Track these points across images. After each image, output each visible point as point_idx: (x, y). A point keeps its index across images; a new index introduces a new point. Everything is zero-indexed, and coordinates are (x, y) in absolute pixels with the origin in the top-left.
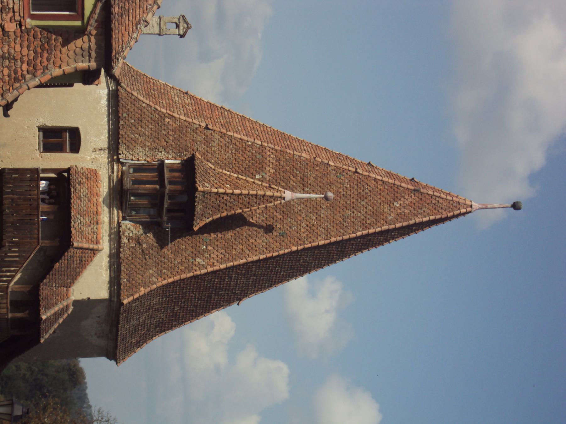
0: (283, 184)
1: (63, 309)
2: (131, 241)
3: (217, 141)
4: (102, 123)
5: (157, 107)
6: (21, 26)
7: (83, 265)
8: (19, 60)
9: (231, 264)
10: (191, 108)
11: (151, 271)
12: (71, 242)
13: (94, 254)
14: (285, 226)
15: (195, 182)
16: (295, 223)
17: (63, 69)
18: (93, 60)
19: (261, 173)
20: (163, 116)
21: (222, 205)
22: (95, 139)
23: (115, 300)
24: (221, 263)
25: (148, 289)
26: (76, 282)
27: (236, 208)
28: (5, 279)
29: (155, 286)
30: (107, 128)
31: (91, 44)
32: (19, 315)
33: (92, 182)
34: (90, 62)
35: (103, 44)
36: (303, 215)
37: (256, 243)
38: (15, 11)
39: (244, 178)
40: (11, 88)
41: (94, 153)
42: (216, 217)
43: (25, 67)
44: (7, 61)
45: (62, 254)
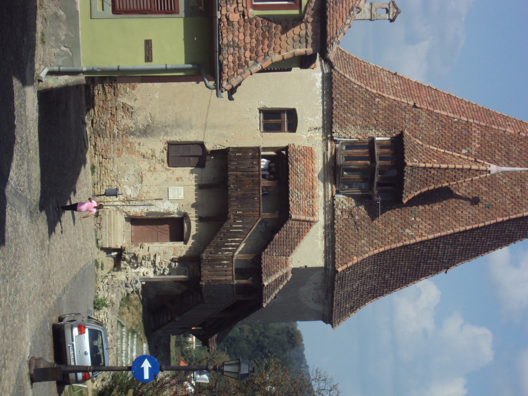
0: (489, 158)
1: (283, 276)
2: (344, 213)
3: (424, 119)
4: (317, 104)
5: (368, 88)
6: (244, 16)
7: (300, 235)
8: (242, 48)
9: (437, 235)
10: (399, 88)
11: (363, 241)
12: (289, 214)
13: (311, 226)
14: (491, 198)
15: (404, 158)
16: (500, 195)
17: (282, 54)
18: (309, 46)
19: (467, 148)
20: (373, 96)
21: (429, 179)
23: (331, 268)
24: (429, 234)
25: (361, 258)
26: (294, 251)
27: (442, 181)
28: (230, 248)
29: (367, 255)
31: (307, 30)
32: (243, 281)
33: (308, 159)
34: (306, 47)
35: (319, 31)
36: (508, 188)
37: (462, 215)
38: (239, 2)
39: (451, 153)
40: (236, 73)
41: (310, 132)
42: (423, 190)
43: (248, 54)
44: (232, 49)
45: (282, 226)
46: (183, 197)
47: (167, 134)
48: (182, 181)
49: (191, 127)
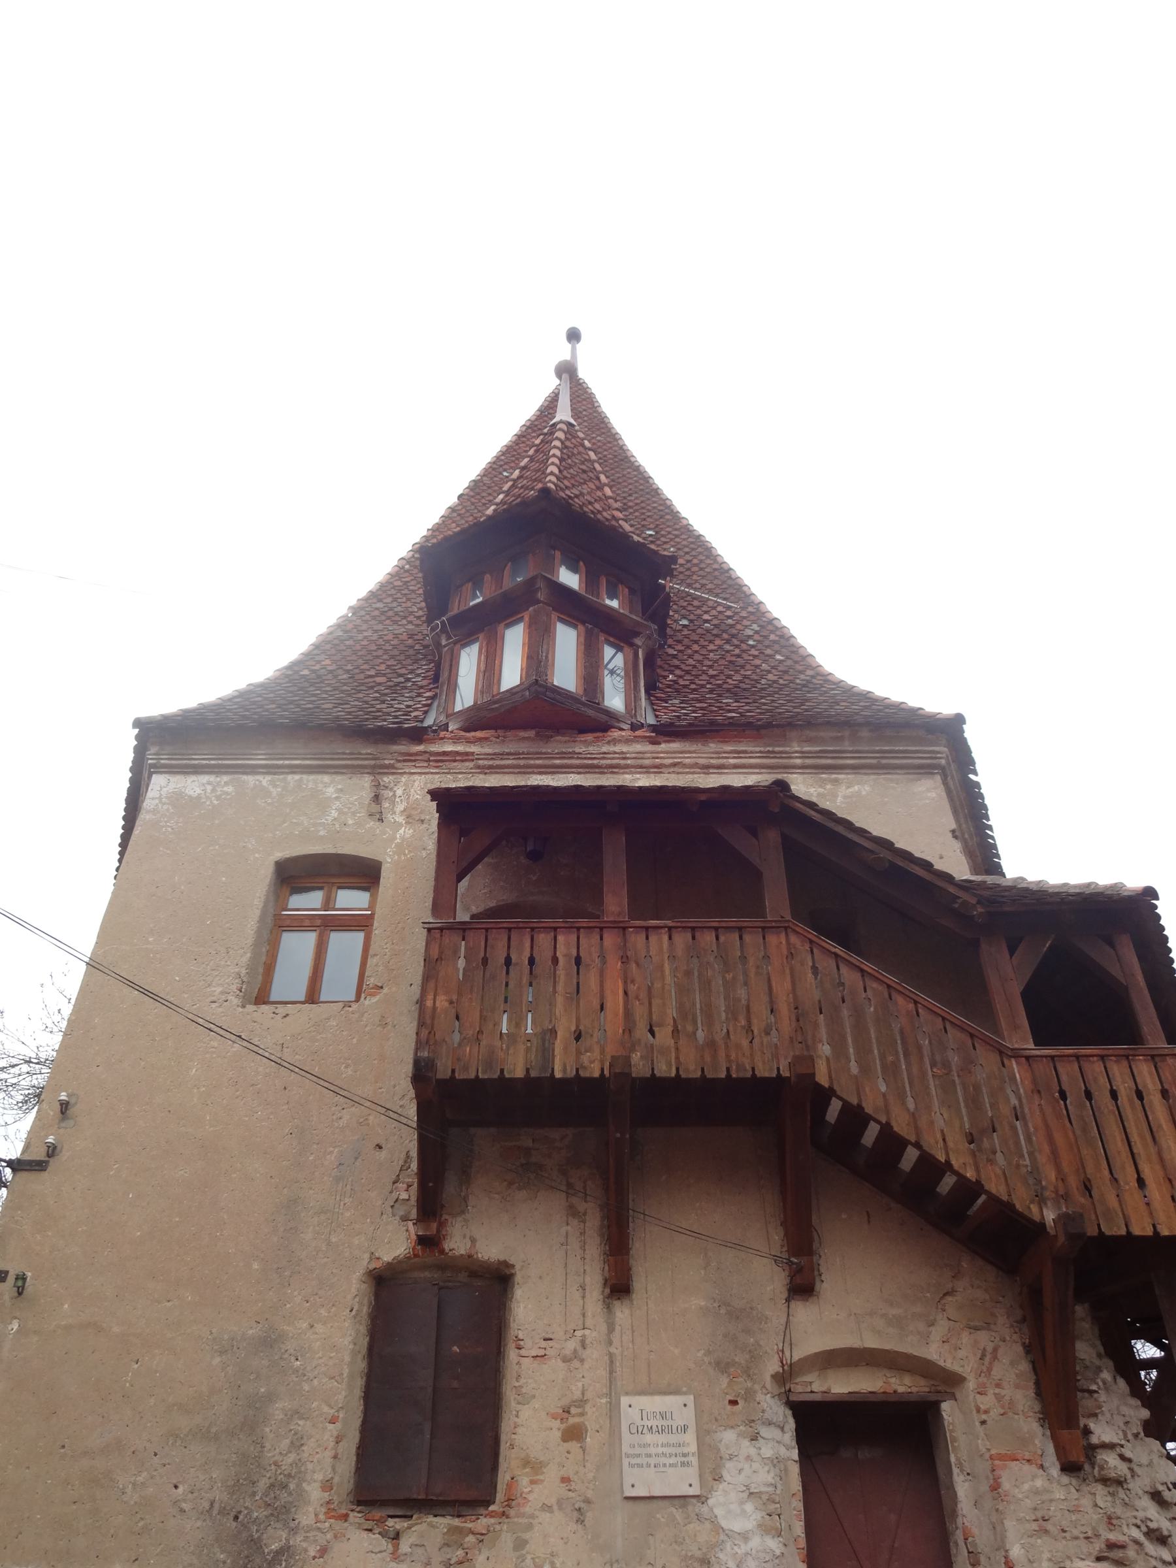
4: (275, 792)
22: (334, 814)
30: (297, 777)
41: (389, 817)
47: (286, 1509)
48: (582, 1402)
49: (269, 1342)
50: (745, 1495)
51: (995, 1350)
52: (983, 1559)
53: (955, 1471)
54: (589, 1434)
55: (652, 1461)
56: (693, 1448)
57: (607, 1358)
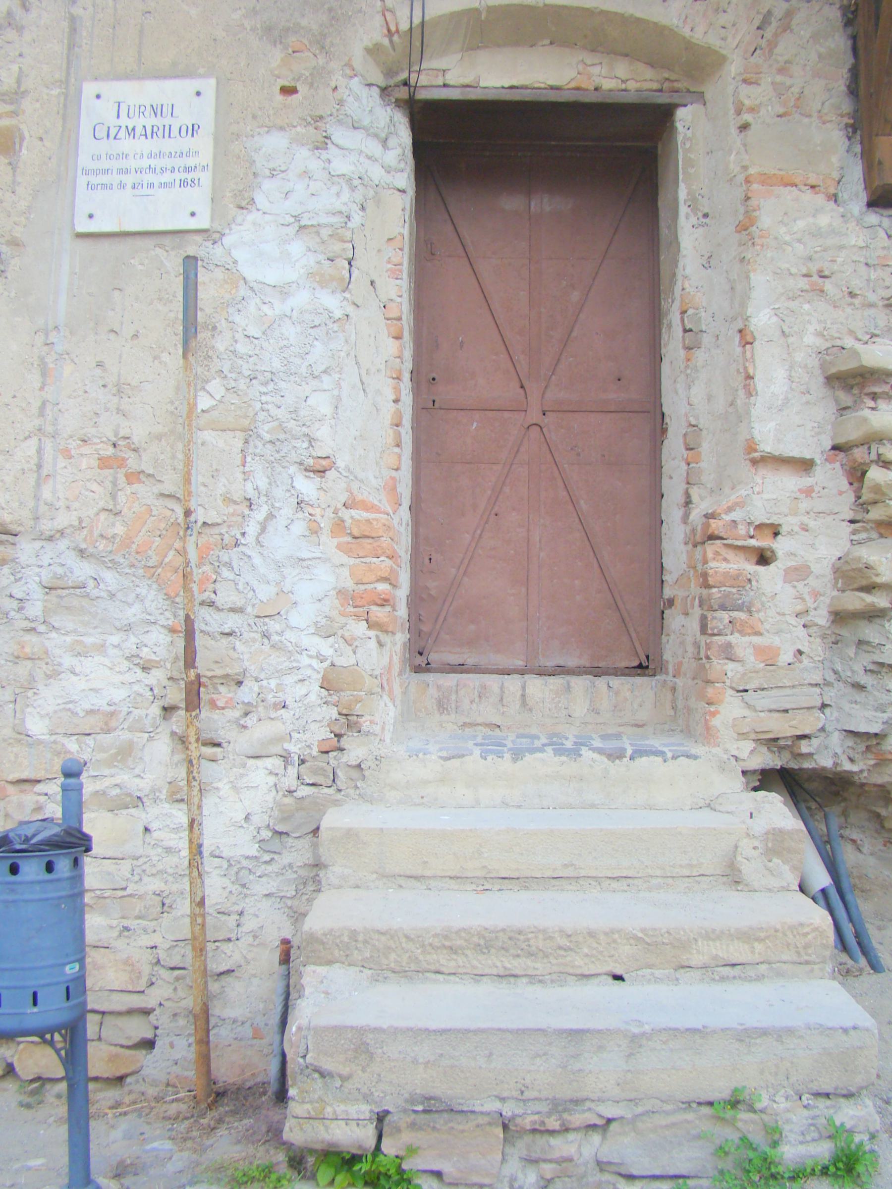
46: (189, 85)
50: (292, 230)
51: (789, 14)
52: (706, 339)
53: (683, 210)
54: (25, 144)
55: (129, 180)
56: (206, 156)
57: (65, 24)
